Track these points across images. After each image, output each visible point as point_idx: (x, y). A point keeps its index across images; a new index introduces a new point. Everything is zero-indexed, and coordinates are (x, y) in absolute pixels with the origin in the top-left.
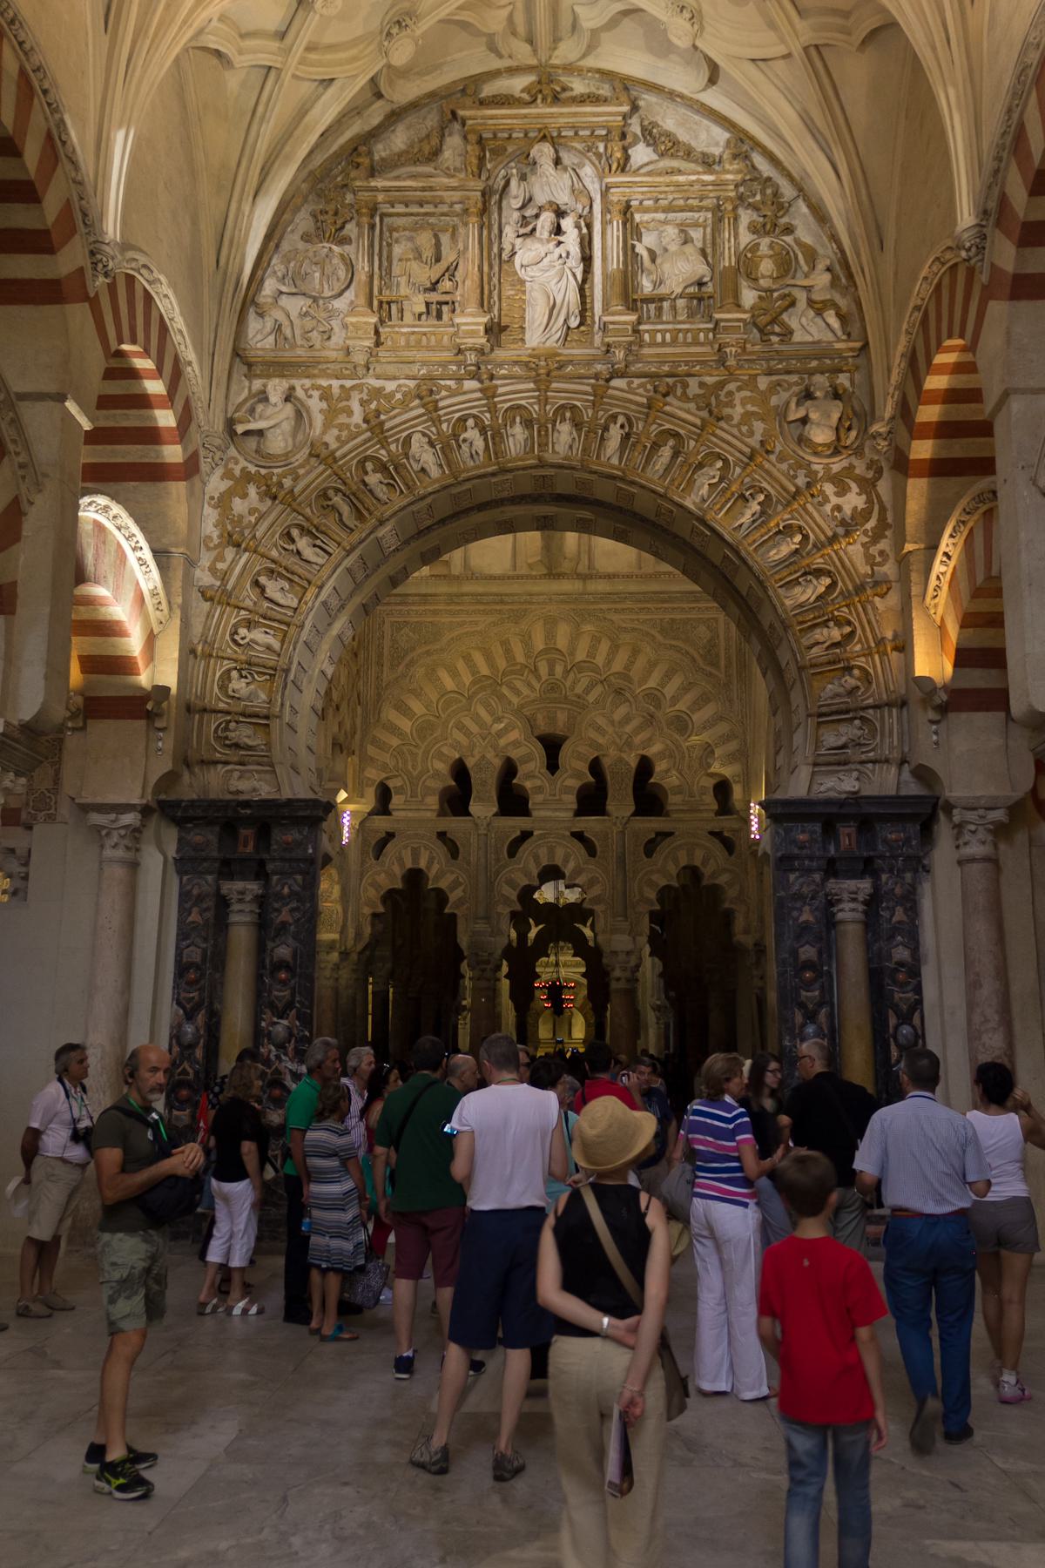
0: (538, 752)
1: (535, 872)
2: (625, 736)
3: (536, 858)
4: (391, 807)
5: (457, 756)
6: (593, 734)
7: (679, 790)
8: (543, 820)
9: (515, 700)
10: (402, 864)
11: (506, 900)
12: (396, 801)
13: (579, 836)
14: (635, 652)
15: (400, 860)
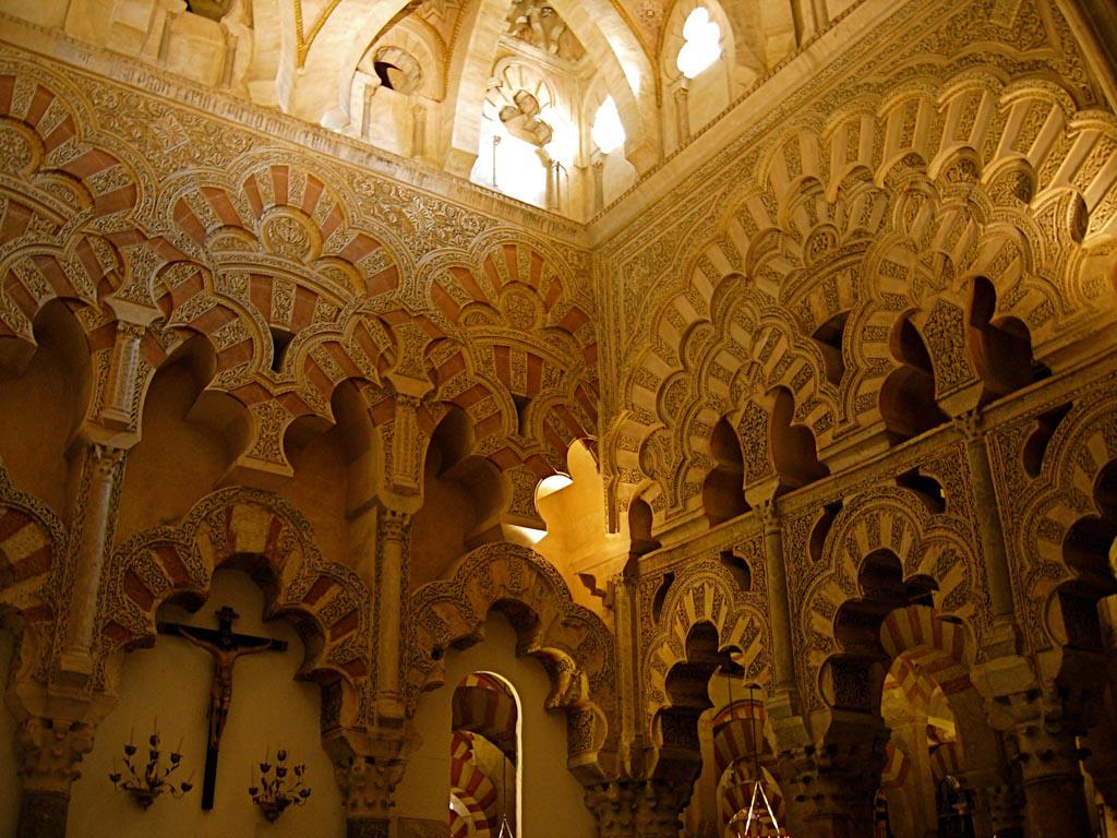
0: (812, 356)
1: (853, 574)
2: (938, 262)
3: (852, 546)
4: (654, 534)
5: (717, 418)
6: (889, 285)
7: (1047, 311)
8: (848, 474)
9: (774, 291)
10: (685, 621)
11: (821, 643)
12: (658, 519)
13: (912, 481)
14: (912, 106)
15: (683, 613)
